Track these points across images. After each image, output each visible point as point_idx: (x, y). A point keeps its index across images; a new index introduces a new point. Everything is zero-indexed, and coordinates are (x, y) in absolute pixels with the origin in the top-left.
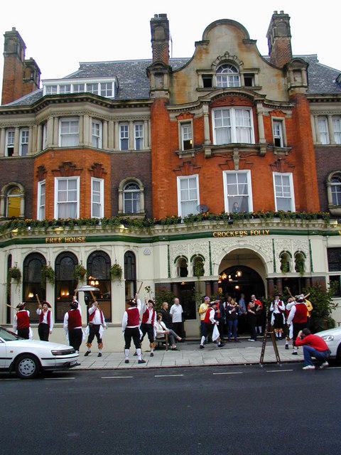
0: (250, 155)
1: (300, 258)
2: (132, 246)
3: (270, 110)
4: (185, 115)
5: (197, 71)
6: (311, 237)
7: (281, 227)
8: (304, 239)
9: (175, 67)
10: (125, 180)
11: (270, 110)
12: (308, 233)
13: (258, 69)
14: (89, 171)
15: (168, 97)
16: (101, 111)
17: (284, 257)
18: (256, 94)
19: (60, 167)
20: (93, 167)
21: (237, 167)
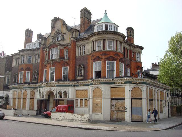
0: (56, 62)
1: (66, 93)
5: (52, 37)
6: (69, 87)
7: (63, 84)
8: (67, 87)
9: (46, 37)
12: (68, 86)
13: (65, 34)
14: (26, 69)
15: (44, 46)
16: (30, 53)
17: (60, 93)
21: (52, 66)
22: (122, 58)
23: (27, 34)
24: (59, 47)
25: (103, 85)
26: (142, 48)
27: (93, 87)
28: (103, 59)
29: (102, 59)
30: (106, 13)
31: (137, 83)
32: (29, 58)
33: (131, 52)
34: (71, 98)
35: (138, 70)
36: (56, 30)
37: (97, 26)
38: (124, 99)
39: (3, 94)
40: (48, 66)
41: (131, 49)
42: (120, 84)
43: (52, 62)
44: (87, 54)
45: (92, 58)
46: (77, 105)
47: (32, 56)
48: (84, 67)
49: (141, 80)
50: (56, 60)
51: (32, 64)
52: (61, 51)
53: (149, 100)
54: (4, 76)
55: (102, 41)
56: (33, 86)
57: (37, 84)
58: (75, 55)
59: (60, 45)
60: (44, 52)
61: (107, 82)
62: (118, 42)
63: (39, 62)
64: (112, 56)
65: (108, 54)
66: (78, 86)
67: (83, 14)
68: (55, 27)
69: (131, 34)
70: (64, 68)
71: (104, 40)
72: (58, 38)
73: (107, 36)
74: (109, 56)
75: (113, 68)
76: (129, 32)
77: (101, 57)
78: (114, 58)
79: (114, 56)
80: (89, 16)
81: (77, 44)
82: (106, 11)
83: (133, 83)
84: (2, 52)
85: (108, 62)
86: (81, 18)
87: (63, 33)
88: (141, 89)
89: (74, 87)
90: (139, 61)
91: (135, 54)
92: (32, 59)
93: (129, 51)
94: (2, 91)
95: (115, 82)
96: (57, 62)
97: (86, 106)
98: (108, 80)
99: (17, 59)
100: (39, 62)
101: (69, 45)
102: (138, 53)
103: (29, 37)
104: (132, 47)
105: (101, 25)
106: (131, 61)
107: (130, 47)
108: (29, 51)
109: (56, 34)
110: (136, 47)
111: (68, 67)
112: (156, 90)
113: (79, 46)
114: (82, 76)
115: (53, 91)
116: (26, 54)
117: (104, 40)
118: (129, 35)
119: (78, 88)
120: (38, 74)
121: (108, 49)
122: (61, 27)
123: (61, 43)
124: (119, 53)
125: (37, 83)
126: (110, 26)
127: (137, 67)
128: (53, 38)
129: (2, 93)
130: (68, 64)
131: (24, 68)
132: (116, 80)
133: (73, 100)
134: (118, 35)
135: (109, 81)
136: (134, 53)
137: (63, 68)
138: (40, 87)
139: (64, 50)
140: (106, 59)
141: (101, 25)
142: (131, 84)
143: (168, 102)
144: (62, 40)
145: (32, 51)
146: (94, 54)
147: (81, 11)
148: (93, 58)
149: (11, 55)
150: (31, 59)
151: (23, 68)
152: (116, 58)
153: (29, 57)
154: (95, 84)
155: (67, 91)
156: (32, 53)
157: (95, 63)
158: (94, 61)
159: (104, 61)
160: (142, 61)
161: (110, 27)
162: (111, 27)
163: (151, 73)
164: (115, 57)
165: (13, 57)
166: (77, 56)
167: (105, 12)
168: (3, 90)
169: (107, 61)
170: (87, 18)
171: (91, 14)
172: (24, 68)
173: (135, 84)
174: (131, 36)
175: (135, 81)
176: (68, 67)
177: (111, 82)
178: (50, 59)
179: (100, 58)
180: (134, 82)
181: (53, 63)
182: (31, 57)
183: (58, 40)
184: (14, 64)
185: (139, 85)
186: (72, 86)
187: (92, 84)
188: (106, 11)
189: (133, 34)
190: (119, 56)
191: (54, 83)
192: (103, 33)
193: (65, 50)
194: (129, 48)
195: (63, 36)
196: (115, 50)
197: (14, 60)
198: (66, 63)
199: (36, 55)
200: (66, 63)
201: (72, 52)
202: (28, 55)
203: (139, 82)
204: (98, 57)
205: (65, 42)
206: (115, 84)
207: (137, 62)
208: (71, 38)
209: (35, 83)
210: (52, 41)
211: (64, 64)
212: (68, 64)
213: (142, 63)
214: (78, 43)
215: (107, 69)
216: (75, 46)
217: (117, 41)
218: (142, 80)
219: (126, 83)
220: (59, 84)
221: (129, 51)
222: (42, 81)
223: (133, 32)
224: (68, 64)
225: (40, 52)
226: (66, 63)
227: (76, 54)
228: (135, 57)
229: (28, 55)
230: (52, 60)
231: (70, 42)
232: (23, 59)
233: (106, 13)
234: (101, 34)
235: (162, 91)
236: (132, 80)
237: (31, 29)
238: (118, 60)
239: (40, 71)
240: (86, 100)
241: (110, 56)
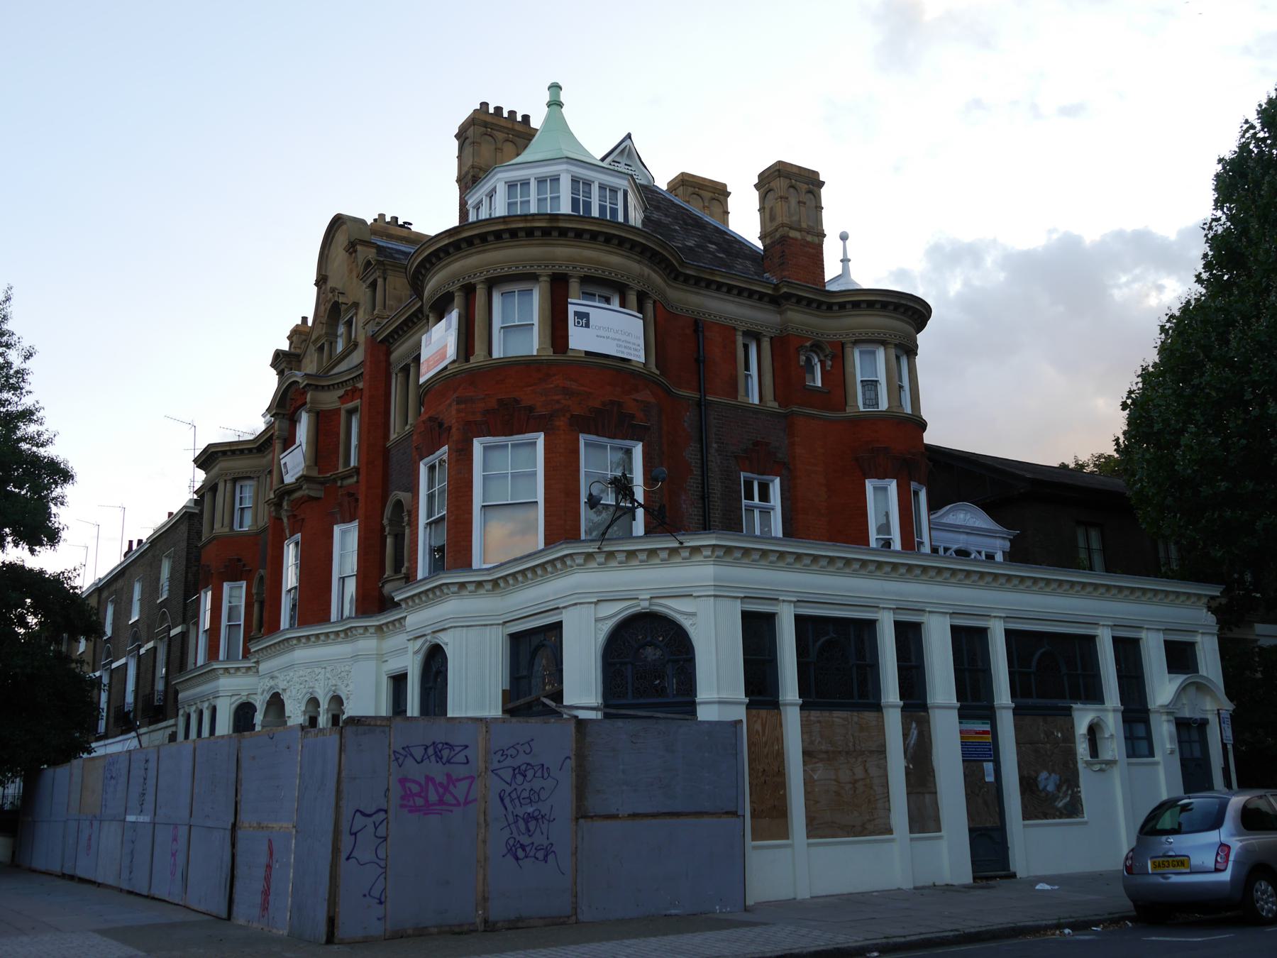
11: (341, 392)
58: (386, 436)
82: (555, 88)
102: (869, 347)
107: (781, 313)
139: (343, 414)
167: (546, 97)
188: (555, 88)
221: (766, 344)
223: (817, 198)
229: (235, 480)
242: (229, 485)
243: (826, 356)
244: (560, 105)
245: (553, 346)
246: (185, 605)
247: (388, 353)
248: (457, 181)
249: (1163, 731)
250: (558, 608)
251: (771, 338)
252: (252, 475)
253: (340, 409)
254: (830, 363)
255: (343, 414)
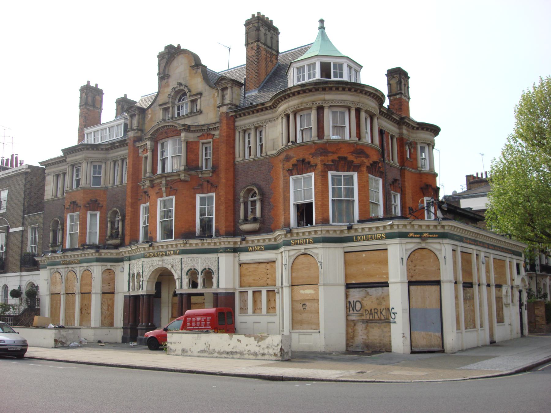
1: (208, 274)
2: (109, 265)
3: (200, 134)
4: (206, 136)
5: (160, 105)
6: (219, 255)
7: (200, 247)
8: (213, 256)
9: (145, 106)
10: (111, 211)
11: (200, 134)
12: (215, 251)
13: (200, 94)
14: (85, 206)
15: (139, 134)
16: (97, 155)
17: (193, 273)
18: (179, 124)
19: (69, 206)
20: (89, 204)
21: (164, 194)
22: (375, 163)
23: (87, 97)
24: (183, 134)
25: (320, 245)
26: (435, 130)
27: (292, 253)
28: (320, 167)
29: (316, 165)
30: (322, 28)
31: (425, 235)
32: (94, 173)
33: (402, 142)
34: (226, 289)
35: (424, 195)
36: (173, 83)
37: (298, 69)
38: (385, 285)
39: (21, 281)
40: (152, 192)
41: (401, 134)
42: (371, 239)
43: (164, 182)
44: (269, 153)
45: (286, 166)
46: (244, 309)
47: (103, 166)
48: (262, 194)
49: (435, 226)
50: (178, 174)
51: (105, 190)
52: (191, 148)
53: (461, 287)
54: (20, 229)
55: (314, 113)
56: (109, 256)
57: (121, 250)
58: (234, 158)
59: (188, 128)
60: (140, 151)
61: (332, 235)
62: (363, 115)
63: (125, 181)
64: (345, 158)
65: (333, 153)
66: (246, 250)
67: (253, 33)
68: (168, 76)
69: (401, 89)
70: (201, 198)
71: (320, 110)
72: (179, 109)
73: (329, 97)
74: (335, 157)
75: (350, 192)
76: (393, 82)
77: (313, 161)
78: (353, 162)
79: (351, 158)
80: (272, 38)
81: (237, 124)
82: (322, 21)
83: (412, 237)
84: (12, 156)
85: (332, 175)
86: (247, 44)
87: (194, 92)
88: (437, 253)
89: (232, 254)
90: (427, 168)
91: (416, 148)
92: (103, 175)
93: (395, 141)
94: (18, 274)
95: (356, 237)
96: (181, 181)
97: (271, 309)
98: (335, 231)
99: (58, 176)
100: (125, 181)
101: (215, 129)
102: (423, 145)
103: (92, 109)
104: (404, 127)
105: (309, 66)
106: (402, 171)
108: (93, 149)
109: (174, 98)
110: (418, 129)
111: (214, 194)
112: (482, 255)
113: (245, 131)
114: (255, 220)
115: (169, 267)
116: (86, 159)
117: (320, 110)
118: (394, 93)
119: (245, 257)
120: (123, 220)
121: (331, 135)
122: (188, 75)
123: (188, 122)
124: (367, 146)
125: (122, 245)
126: (335, 65)
127: (422, 189)
128: (166, 110)
129: (18, 278)
130: (212, 184)
131: (81, 202)
132: (360, 230)
133: (233, 294)
134: (361, 92)
135: (338, 232)
136: (413, 145)
137: (198, 197)
138: (130, 259)
139: (201, 145)
140: (328, 167)
141: (309, 66)
142: (404, 240)
143: (520, 292)
144: (192, 114)
145: (102, 149)
146: (291, 153)
147: (248, 24)
148: (289, 165)
149: (41, 163)
150: (100, 173)
151: (78, 202)
152: (357, 161)
153: (95, 167)
154: (297, 244)
155: (214, 268)
156: (104, 156)
157: (295, 180)
158: (291, 172)
159: (322, 171)
160: (436, 171)
161: (335, 68)
162: (341, 68)
163: (465, 204)
164: (355, 160)
165: (46, 171)
166: (238, 159)
167: (318, 25)
168: (21, 271)
169: (330, 174)
170: (265, 44)
171: (276, 31)
172: (81, 202)
173: (418, 240)
174: (401, 93)
175: (417, 229)
176: (214, 194)
177: (346, 234)
178: (159, 171)
179: (309, 163)
180: (415, 233)
181: (167, 184)
182: (100, 167)
183: (179, 114)
184: (49, 192)
185: (430, 241)
186: (226, 250)
187: (287, 244)
188: (322, 21)
189: (408, 87)
190: (367, 156)
191: (172, 245)
192: (317, 90)
193: (203, 144)
194: (397, 130)
195: (193, 102)
196: (355, 138)
197: (50, 180)
198: (208, 182)
199: (115, 162)
200: (205, 184)
201: (223, 148)
202: (92, 162)
203: (430, 233)
204: (303, 160)
205: (201, 120)
206: (357, 240)
207: (421, 174)
208: (218, 107)
209: (116, 247)
210: (161, 118)
211: (201, 185)
212: (212, 184)
213: (435, 175)
214: (243, 122)
215: (330, 198)
216: (232, 130)
217: (358, 111)
218: (439, 227)
219: (389, 236)
220: (188, 247)
221: (395, 141)
222: (135, 240)
224: (212, 186)
225: (127, 151)
226: (208, 182)
227: (237, 156)
228: (414, 157)
229: (92, 162)
230: (164, 175)
231: (217, 120)
232: (77, 176)
233: (322, 28)
234: (310, 91)
235: (498, 257)
236: (408, 227)
237: (97, 85)
238: (364, 169)
239: (129, 210)
240: (271, 293)
241: (339, 158)
242: (89, 165)
243: (412, 147)
244: (324, 28)
245: (357, 137)
246: (24, 218)
247: (234, 122)
248: (245, 45)
249: (517, 294)
250: (385, 244)
251: (397, 138)
252: (102, 161)
253: (199, 142)
254: (413, 150)
255: (201, 145)
